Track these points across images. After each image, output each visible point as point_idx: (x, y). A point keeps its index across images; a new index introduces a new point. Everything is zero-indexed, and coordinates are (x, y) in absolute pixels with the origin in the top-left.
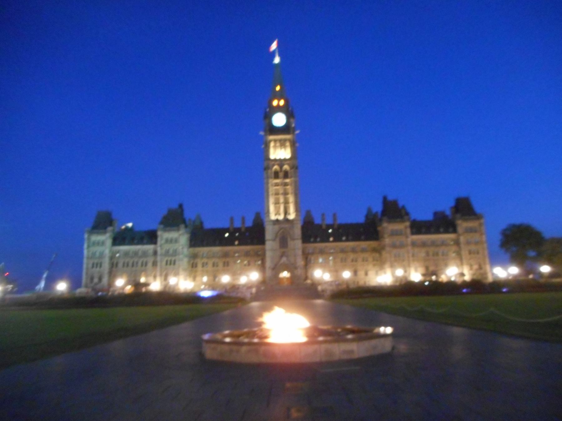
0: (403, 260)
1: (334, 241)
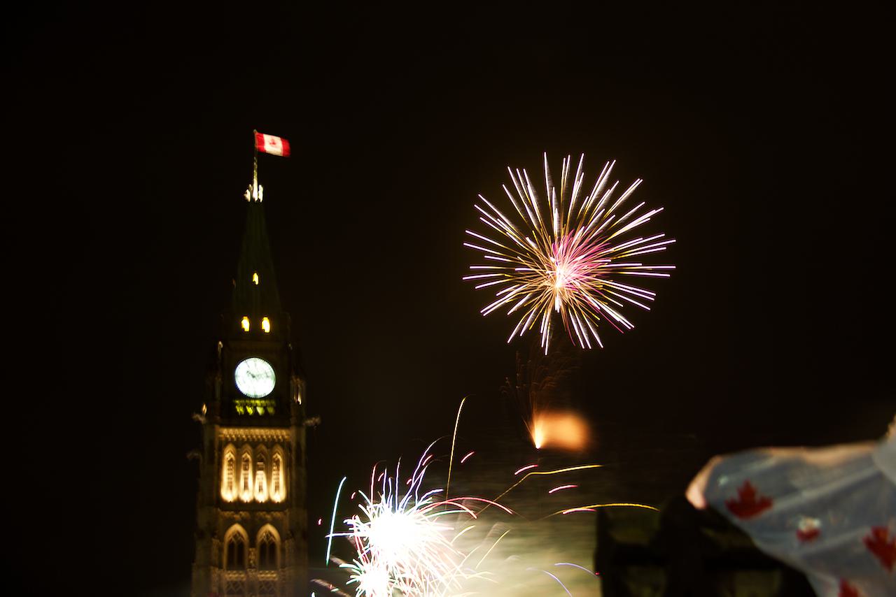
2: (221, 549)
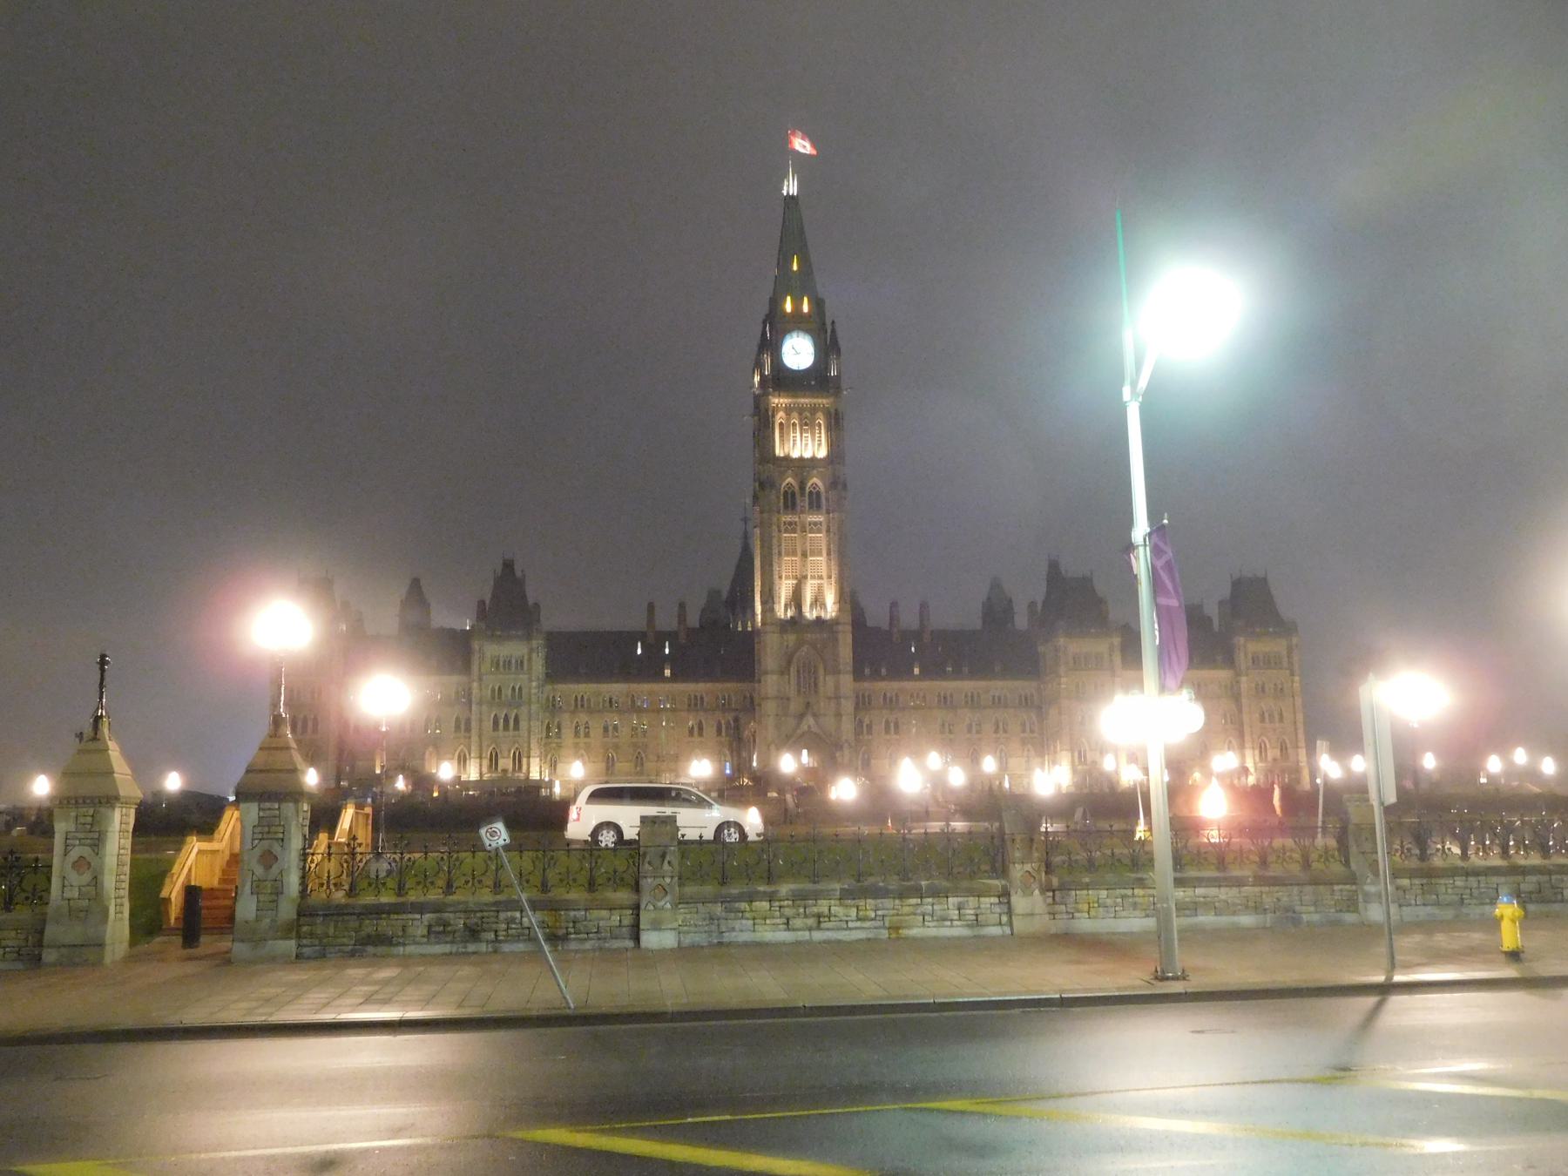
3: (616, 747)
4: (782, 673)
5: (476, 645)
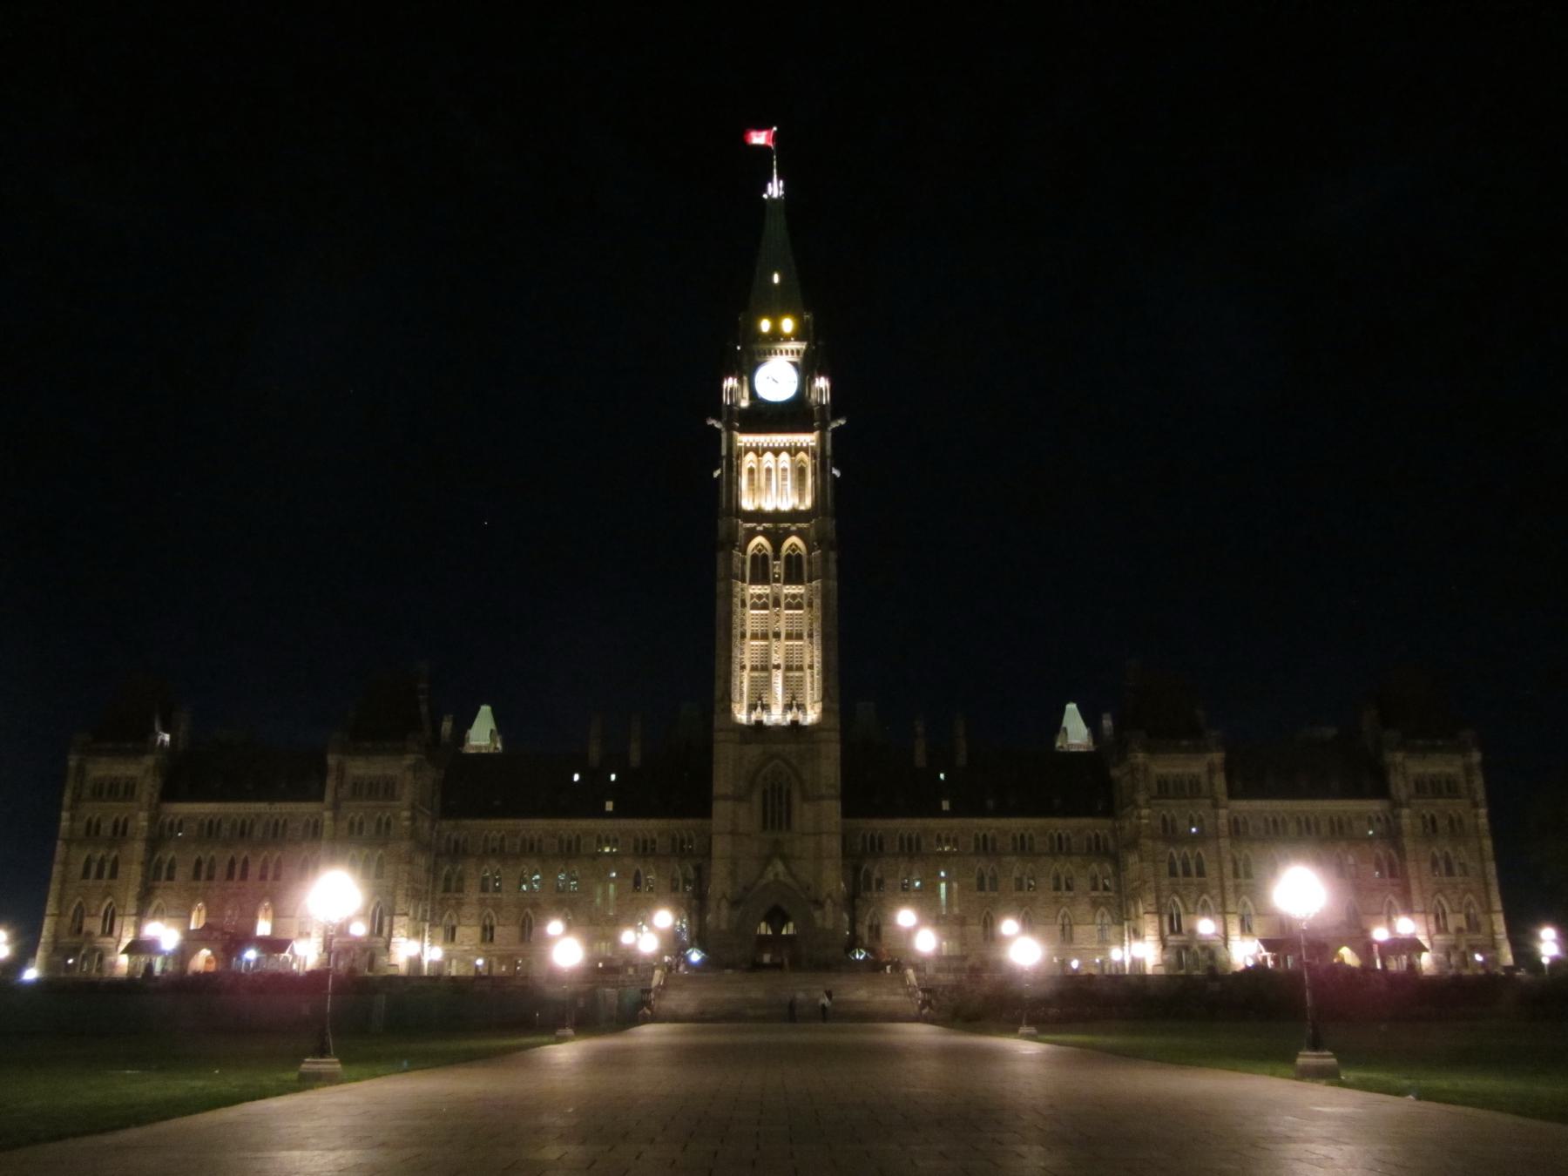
0: (1203, 889)
1: (954, 813)
2: (744, 562)
3: (498, 907)
4: (737, 798)
5: (332, 760)
